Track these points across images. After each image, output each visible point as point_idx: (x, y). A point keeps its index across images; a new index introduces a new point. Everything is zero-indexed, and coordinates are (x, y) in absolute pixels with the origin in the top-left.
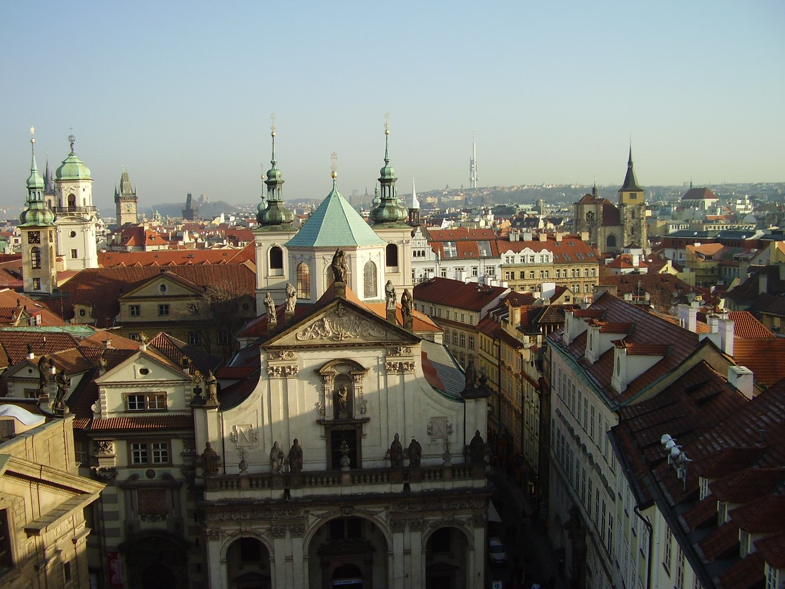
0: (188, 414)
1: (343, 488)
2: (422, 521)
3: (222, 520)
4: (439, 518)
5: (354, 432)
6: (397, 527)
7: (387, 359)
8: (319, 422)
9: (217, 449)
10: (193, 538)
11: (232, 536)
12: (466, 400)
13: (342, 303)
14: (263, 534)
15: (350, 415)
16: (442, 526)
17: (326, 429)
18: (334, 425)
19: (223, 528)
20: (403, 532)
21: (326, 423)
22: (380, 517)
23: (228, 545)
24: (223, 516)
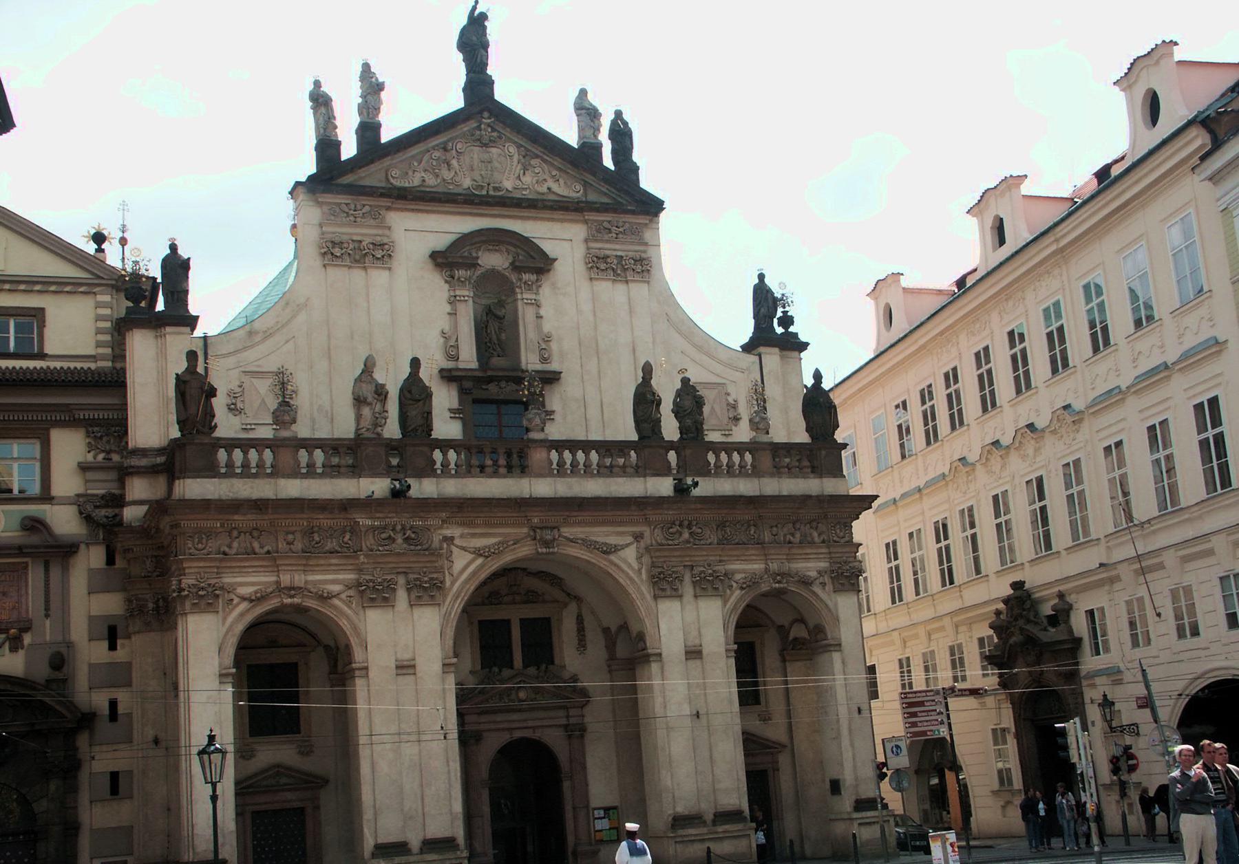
0: (101, 364)
1: (534, 480)
2: (721, 568)
3: (225, 553)
4: (756, 566)
6: (664, 583)
8: (448, 376)
10: (100, 701)
11: (255, 600)
12: (762, 349)
13: (490, 111)
14: (337, 596)
16: (765, 588)
17: (463, 392)
19: (228, 580)
20: (681, 596)
21: (460, 374)
23: (240, 628)
24: (230, 547)
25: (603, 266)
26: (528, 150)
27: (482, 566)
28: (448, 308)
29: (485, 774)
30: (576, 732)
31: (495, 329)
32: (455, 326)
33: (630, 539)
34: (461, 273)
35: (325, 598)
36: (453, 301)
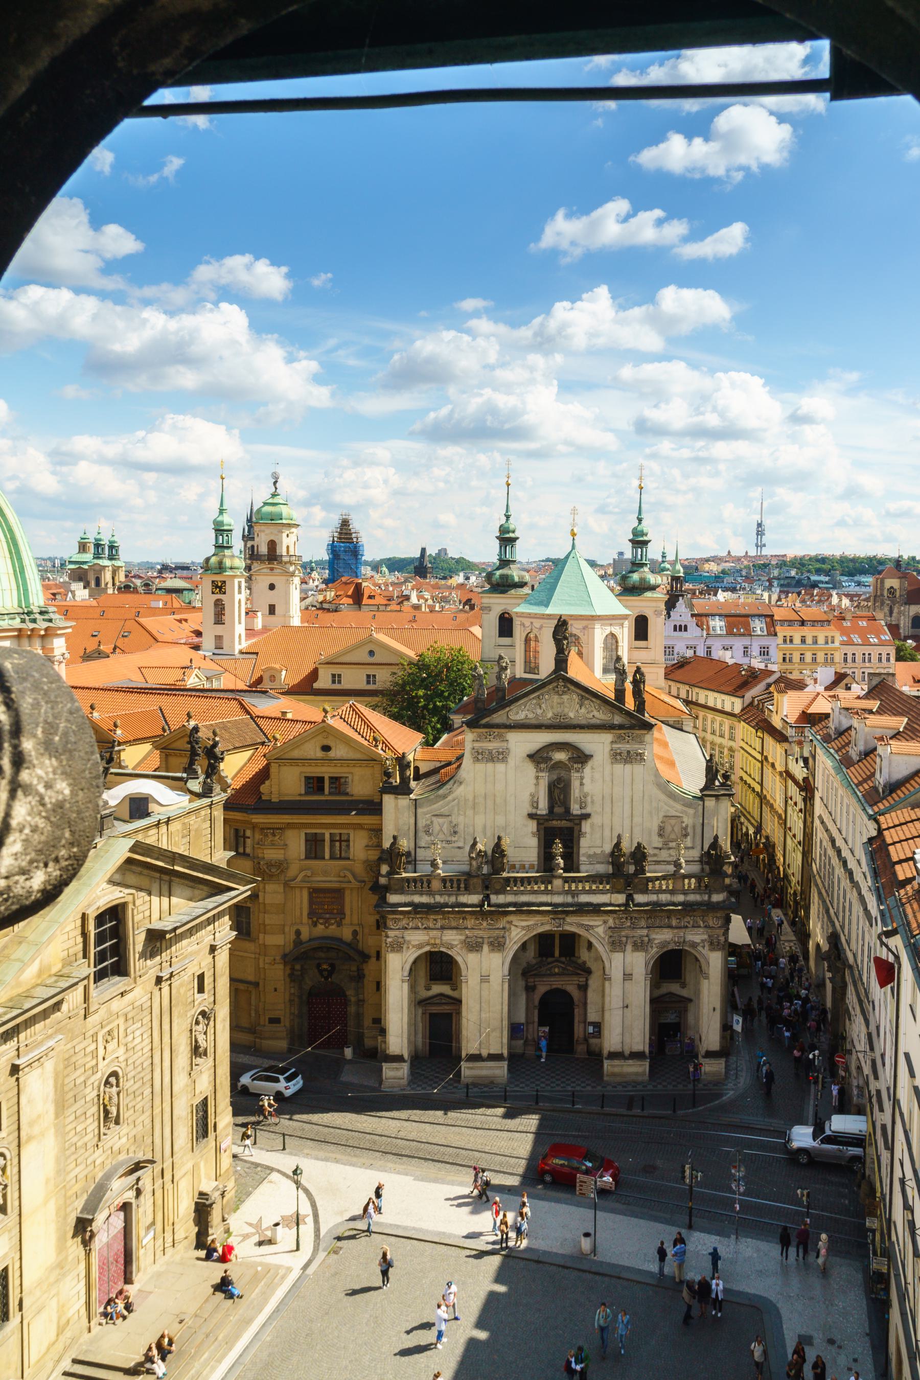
5: (571, 831)
6: (616, 945)
7: (615, 746)
9: (405, 844)
11: (420, 946)
15: (568, 810)
17: (538, 824)
18: (547, 820)
20: (624, 952)
22: (597, 933)
25: (618, 757)
26: (582, 696)
27: (525, 935)
28: (535, 781)
29: (537, 1002)
30: (584, 988)
31: (559, 791)
32: (537, 791)
33: (601, 923)
34: (543, 766)
35: (451, 947)
36: (537, 778)
